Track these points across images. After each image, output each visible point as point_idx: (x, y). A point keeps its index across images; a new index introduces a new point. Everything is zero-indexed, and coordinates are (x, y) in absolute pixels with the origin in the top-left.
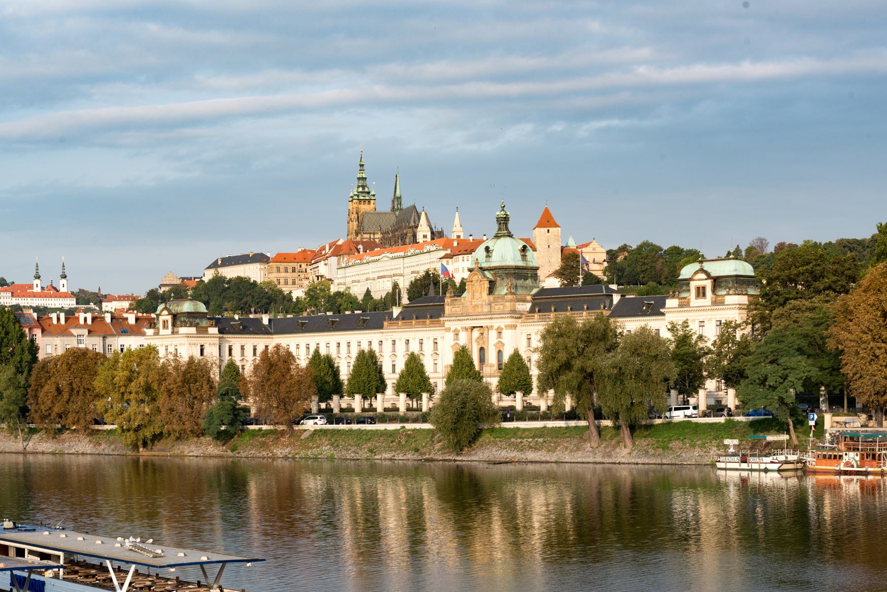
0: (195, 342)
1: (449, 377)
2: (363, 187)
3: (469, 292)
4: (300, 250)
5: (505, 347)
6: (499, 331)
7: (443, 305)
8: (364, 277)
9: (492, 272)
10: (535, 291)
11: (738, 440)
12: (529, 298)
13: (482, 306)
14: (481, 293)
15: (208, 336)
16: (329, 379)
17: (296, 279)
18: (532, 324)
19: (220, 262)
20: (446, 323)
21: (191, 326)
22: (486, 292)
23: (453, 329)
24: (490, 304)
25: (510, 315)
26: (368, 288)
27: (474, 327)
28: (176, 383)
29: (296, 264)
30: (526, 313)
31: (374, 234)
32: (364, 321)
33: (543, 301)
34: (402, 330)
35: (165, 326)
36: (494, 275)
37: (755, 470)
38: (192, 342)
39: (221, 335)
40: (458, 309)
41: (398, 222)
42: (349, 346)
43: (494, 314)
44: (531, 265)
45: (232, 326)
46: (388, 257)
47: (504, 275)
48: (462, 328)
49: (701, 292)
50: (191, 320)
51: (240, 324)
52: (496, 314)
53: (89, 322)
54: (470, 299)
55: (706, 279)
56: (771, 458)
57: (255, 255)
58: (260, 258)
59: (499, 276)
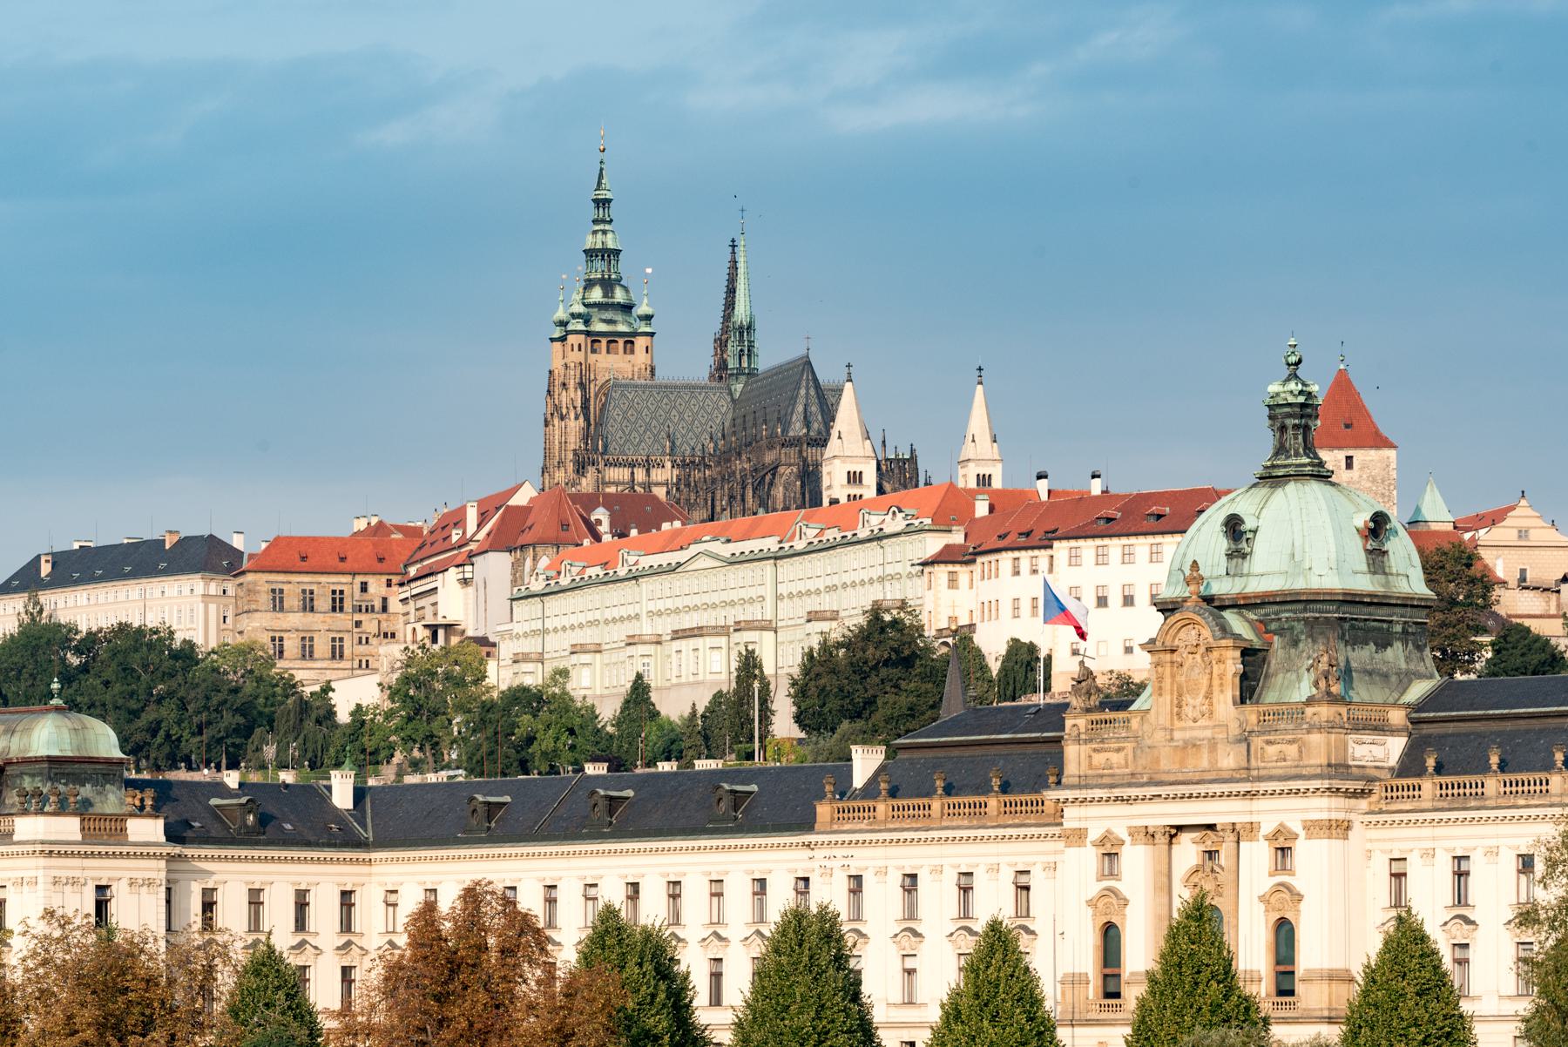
0: (77, 874)
1: (1142, 1021)
2: (608, 285)
4: (361, 525)
5: (1303, 906)
6: (1281, 843)
7: (1058, 740)
8: (620, 632)
9: (1252, 616)
10: (1418, 690)
12: (1397, 717)
13: (1213, 745)
15: (125, 850)
16: (659, 1022)
17: (346, 637)
18: (1413, 817)
19: (46, 569)
20: (1069, 812)
21: (61, 810)
22: (1230, 691)
23: (1095, 834)
24: (1245, 739)
25: (1326, 784)
26: (639, 677)
27: (1180, 828)
28: (74, 1033)
29: (346, 579)
30: (1385, 775)
31: (648, 466)
32: (738, 798)
33: (1451, 728)
34: (888, 836)
36: (1262, 626)
38: (63, 874)
39: (177, 850)
40: (1116, 758)
41: (740, 422)
42: (674, 897)
43: (1260, 779)
45: (214, 813)
46: (716, 557)
47: (1299, 626)
48: (1133, 832)
50: (62, 788)
51: (247, 808)
52: (1271, 778)
54: (1164, 720)
59: (1280, 632)
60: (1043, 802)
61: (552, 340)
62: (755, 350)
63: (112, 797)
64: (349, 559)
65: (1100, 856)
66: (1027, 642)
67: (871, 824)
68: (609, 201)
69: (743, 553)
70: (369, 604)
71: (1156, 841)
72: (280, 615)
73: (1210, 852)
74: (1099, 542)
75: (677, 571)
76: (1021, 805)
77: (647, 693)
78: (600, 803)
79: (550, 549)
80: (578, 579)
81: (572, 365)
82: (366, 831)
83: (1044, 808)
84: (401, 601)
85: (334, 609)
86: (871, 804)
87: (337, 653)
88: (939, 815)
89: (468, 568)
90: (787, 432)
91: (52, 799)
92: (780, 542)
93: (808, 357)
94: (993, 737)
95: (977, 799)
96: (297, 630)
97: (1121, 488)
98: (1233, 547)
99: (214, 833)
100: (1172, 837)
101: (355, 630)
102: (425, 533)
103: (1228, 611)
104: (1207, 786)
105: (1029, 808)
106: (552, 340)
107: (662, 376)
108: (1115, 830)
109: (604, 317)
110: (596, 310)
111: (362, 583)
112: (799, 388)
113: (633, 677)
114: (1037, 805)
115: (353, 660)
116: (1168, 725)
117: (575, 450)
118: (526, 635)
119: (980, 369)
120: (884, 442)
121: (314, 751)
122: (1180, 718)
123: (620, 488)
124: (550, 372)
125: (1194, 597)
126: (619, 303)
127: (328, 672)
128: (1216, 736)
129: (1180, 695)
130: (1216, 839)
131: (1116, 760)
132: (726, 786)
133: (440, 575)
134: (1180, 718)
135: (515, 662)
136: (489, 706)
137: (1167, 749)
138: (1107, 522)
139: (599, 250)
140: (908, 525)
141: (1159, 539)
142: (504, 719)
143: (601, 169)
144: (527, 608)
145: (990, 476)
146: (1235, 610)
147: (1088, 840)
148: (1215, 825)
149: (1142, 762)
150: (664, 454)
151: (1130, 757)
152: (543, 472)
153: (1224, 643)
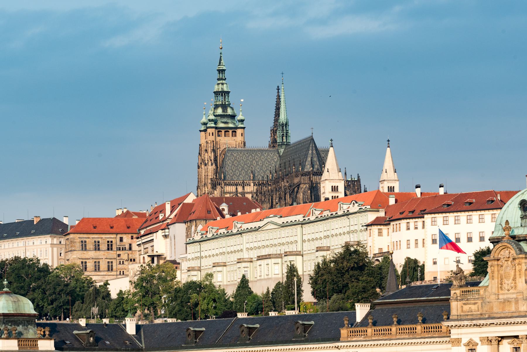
2: (224, 107)
3: (493, 278)
4: (119, 212)
7: (448, 300)
8: (234, 257)
13: (517, 301)
14: (514, 279)
17: (114, 261)
20: (453, 331)
21: (9, 337)
23: (465, 340)
26: (244, 276)
27: (503, 338)
29: (114, 236)
31: (243, 185)
32: (306, 327)
34: (372, 343)
40: (473, 307)
45: (75, 337)
50: (9, 327)
51: (89, 335)
54: (495, 290)
57: (43, 221)
60: (441, 327)
61: (201, 131)
62: (289, 134)
63: (31, 331)
64: (115, 227)
65: (467, 350)
66: (414, 259)
67: (365, 338)
68: (224, 70)
69: (287, 222)
70: (124, 247)
71: (492, 344)
72: (85, 252)
73: (516, 348)
74: (444, 215)
75: (259, 230)
76: (432, 329)
77: (247, 284)
78: (245, 330)
79: (203, 222)
80: (215, 234)
81: (210, 142)
82: (142, 344)
83: (442, 330)
84: (137, 245)
85: (108, 249)
86: (365, 329)
87: (110, 268)
88: (395, 334)
89: (167, 230)
90: (304, 169)
91: (5, 332)
92: (304, 217)
93: (312, 137)
94: (418, 299)
95: (412, 326)
96: (92, 259)
97: (452, 191)
98: (524, 214)
99: (75, 346)
100: (499, 341)
101: (118, 258)
102: (147, 215)
103: (522, 242)
104: (514, 319)
105: (435, 330)
106: (201, 131)
107: (249, 146)
108: (473, 339)
109: (223, 121)
110: (219, 118)
111: (120, 238)
112: (309, 150)
113: (241, 277)
114: (439, 328)
115: (117, 271)
116: (497, 292)
117: (211, 179)
118: (193, 259)
119: (388, 141)
120: (345, 173)
121: (102, 311)
122: (502, 289)
123: (231, 195)
124: (200, 145)
125: (507, 236)
126: (229, 115)
127: (106, 276)
128: (518, 297)
129: (502, 279)
130: (519, 342)
131: (474, 308)
132: (301, 322)
133: (155, 234)
134: (502, 289)
135: (188, 271)
136: (178, 290)
137: (496, 303)
138: (448, 206)
139: (220, 92)
140: (360, 209)
141: (470, 213)
142: (185, 295)
143: (221, 57)
144: (193, 247)
145: (394, 187)
146: (525, 242)
147: (462, 343)
148: (518, 336)
149: (485, 309)
150: (250, 180)
151: (480, 307)
152: (197, 189)
153: (521, 256)
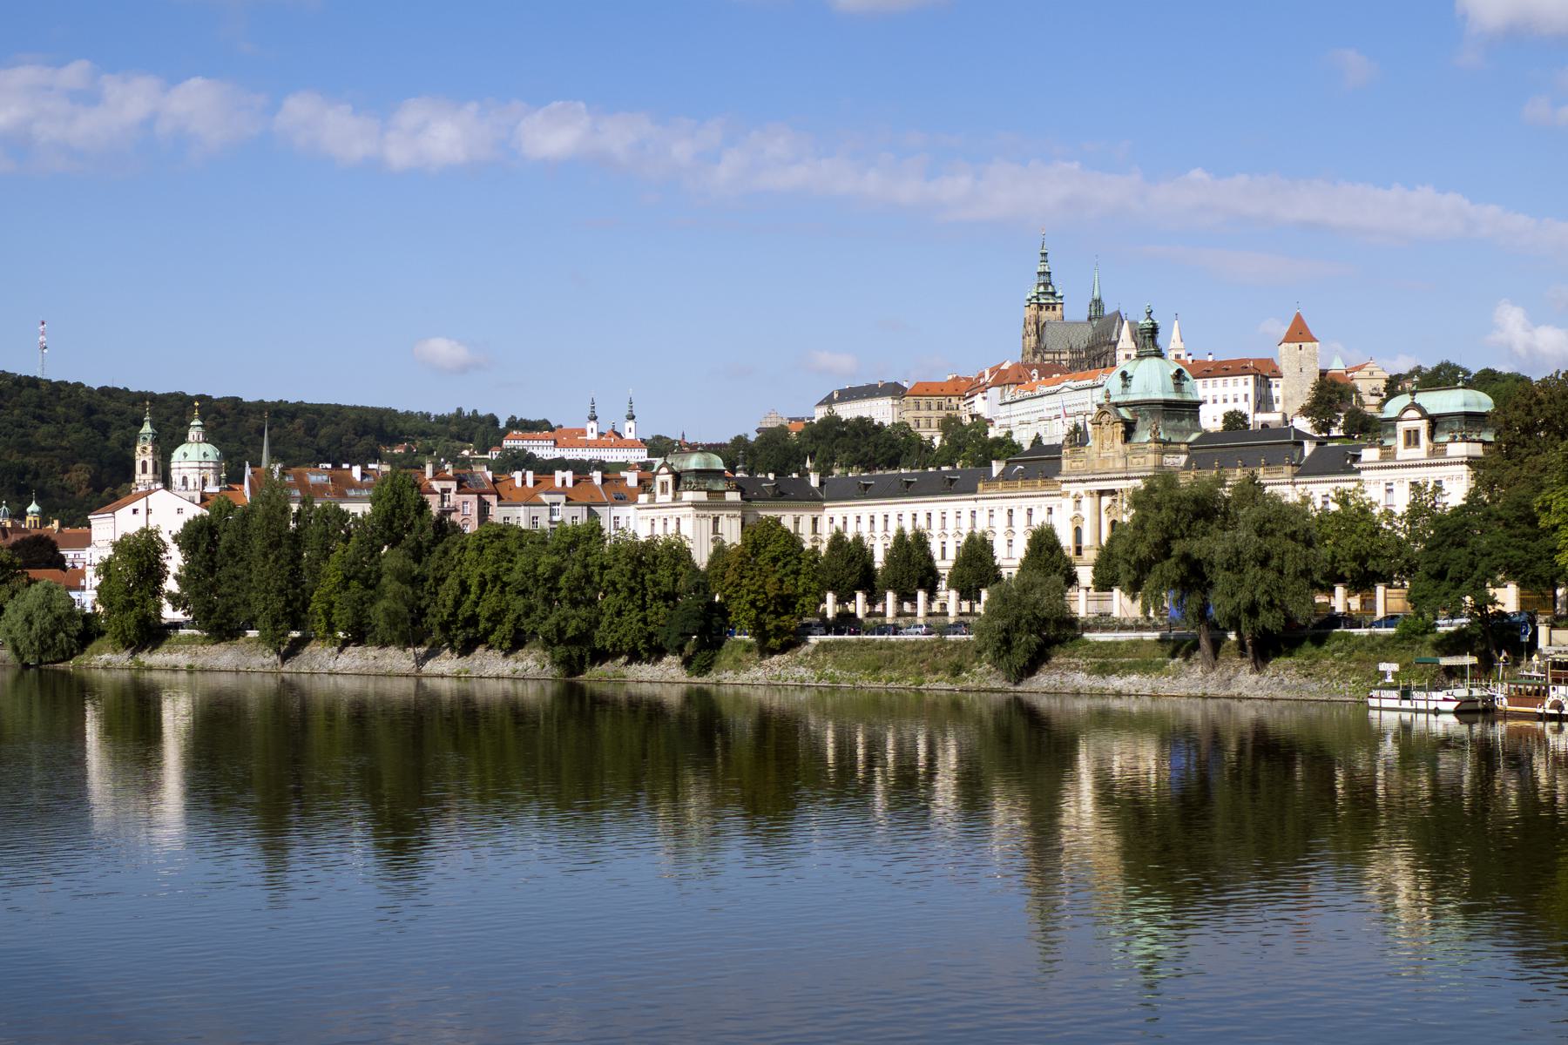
4: (950, 377)
7: (1060, 458)
10: (1194, 437)
11: (1398, 665)
13: (1114, 459)
19: (836, 396)
23: (1072, 494)
26: (1038, 434)
31: (1060, 353)
35: (664, 490)
36: (1133, 413)
37: (1422, 711)
40: (1080, 464)
41: (1095, 336)
43: (1130, 472)
44: (1189, 398)
47: (1147, 413)
48: (1086, 492)
49: (1412, 438)
52: (1134, 471)
53: (569, 484)
54: (1097, 450)
55: (1420, 419)
56: (1445, 692)
57: (886, 385)
58: (894, 391)
